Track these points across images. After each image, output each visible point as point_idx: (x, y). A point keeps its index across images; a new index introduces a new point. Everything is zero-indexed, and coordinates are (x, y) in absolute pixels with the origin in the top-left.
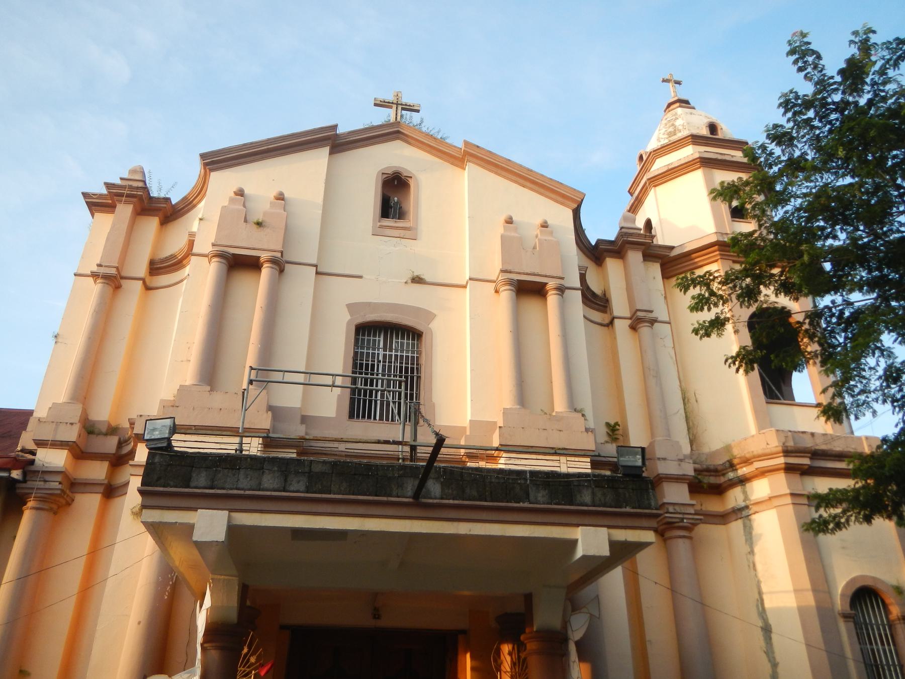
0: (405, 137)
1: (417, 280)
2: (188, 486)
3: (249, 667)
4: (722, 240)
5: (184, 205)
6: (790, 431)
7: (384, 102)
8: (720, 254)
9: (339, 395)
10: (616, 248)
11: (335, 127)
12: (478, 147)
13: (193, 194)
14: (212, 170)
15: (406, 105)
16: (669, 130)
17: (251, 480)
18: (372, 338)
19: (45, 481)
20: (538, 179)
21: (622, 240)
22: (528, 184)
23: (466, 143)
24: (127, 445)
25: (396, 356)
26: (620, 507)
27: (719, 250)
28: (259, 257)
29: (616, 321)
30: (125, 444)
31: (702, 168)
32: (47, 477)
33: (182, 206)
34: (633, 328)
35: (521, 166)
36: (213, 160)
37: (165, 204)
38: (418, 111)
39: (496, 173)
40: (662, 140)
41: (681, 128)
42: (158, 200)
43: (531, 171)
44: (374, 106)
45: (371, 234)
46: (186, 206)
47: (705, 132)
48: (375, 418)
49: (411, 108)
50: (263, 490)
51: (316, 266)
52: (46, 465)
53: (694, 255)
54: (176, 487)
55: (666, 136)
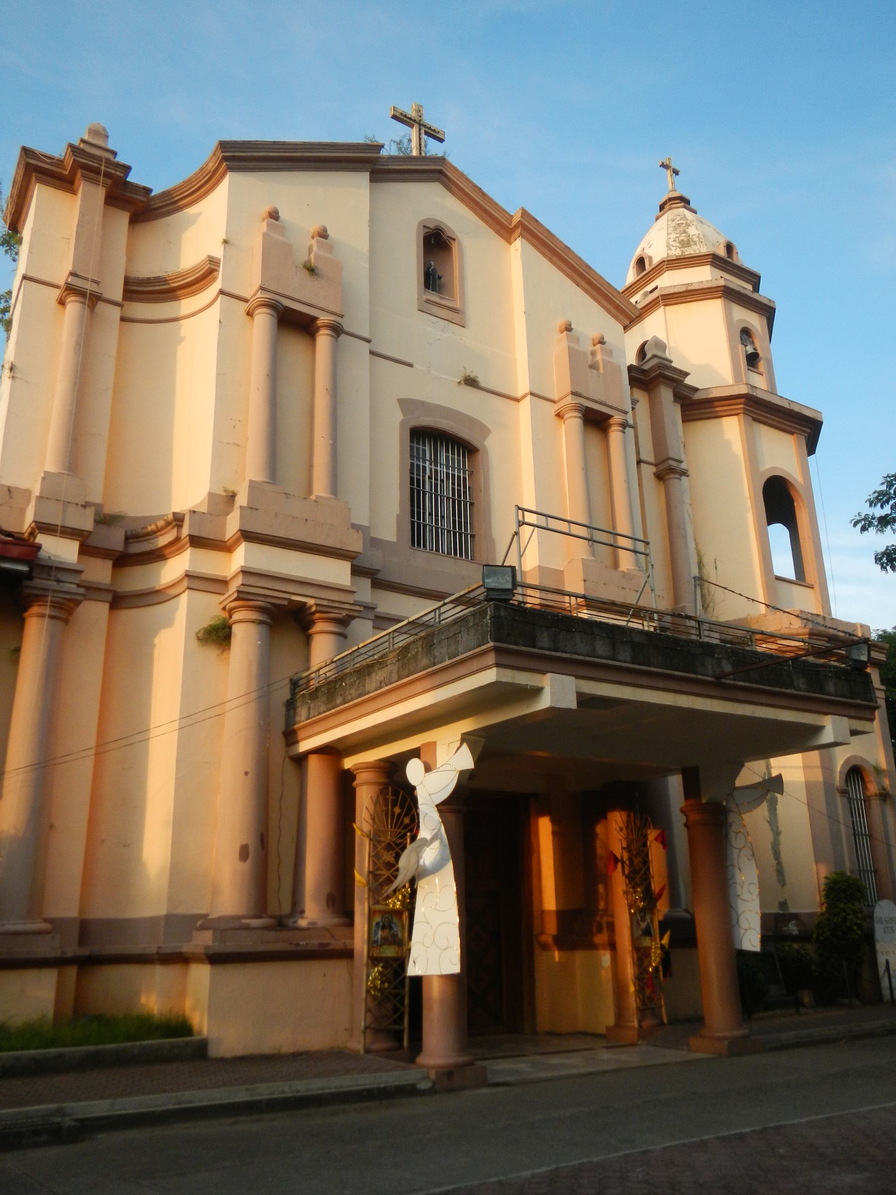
0: (447, 181)
1: (471, 382)
2: (534, 647)
3: (404, 829)
4: (751, 393)
5: (163, 204)
6: (809, 613)
7: (405, 116)
8: (744, 409)
9: (398, 515)
10: (647, 379)
12: (537, 221)
13: (181, 191)
14: (230, 169)
15: (430, 128)
16: (681, 238)
17: (586, 645)
18: (421, 447)
19: (58, 581)
20: (595, 280)
21: (657, 373)
22: (583, 284)
23: (524, 213)
24: (138, 542)
25: (448, 474)
26: (854, 699)
27: (744, 404)
28: (315, 319)
29: (643, 465)
30: (136, 540)
31: (723, 298)
32: (62, 576)
33: (160, 205)
34: (660, 477)
35: (580, 259)
36: (235, 154)
37: (145, 197)
38: (441, 140)
39: (550, 260)
40: (674, 248)
41: (696, 239)
42: (135, 188)
43: (590, 268)
44: (392, 118)
45: (416, 307)
46: (167, 205)
47: (722, 252)
48: (425, 546)
49: (434, 134)
50: (598, 657)
52: (52, 558)
53: (716, 403)
54: (525, 646)
55: (678, 245)
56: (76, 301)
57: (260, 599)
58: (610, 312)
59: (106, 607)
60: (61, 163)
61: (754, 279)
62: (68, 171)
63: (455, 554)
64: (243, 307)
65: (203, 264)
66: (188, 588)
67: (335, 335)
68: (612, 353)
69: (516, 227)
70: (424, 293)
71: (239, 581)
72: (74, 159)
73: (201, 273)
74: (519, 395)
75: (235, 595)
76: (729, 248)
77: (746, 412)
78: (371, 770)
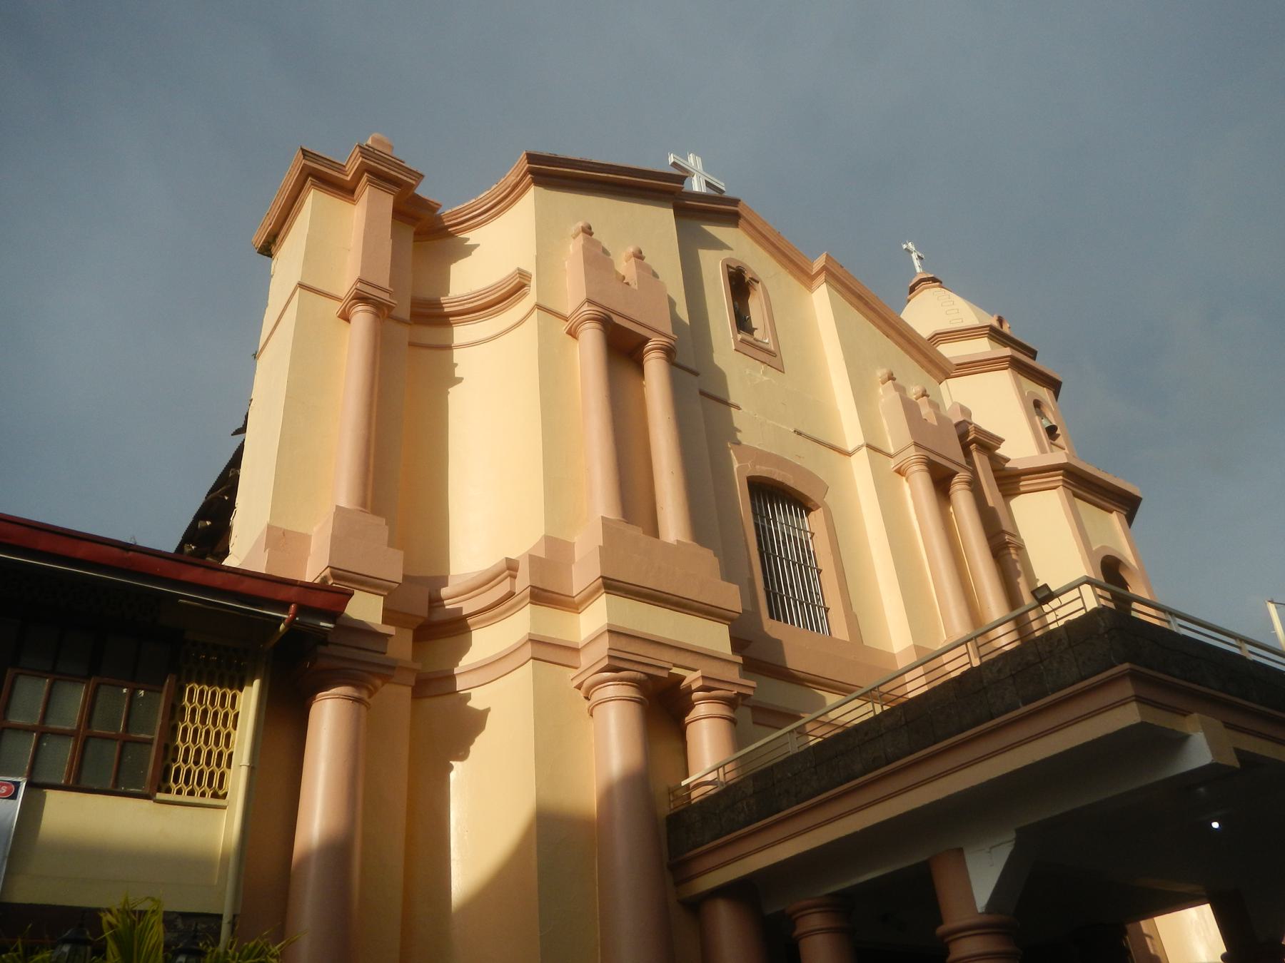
8: (1063, 481)
12: (842, 267)
27: (1063, 476)
51: (696, 374)
56: (366, 311)
57: (635, 667)
58: (922, 366)
59: (407, 691)
60: (341, 167)
61: (1032, 353)
62: (349, 178)
63: (812, 629)
64: (564, 327)
65: (511, 277)
68: (939, 407)
69: (818, 273)
70: (739, 333)
71: (604, 646)
72: (362, 161)
73: (505, 290)
74: (850, 448)
75: (606, 662)
76: (1000, 321)
77: (1066, 485)
78: (822, 909)
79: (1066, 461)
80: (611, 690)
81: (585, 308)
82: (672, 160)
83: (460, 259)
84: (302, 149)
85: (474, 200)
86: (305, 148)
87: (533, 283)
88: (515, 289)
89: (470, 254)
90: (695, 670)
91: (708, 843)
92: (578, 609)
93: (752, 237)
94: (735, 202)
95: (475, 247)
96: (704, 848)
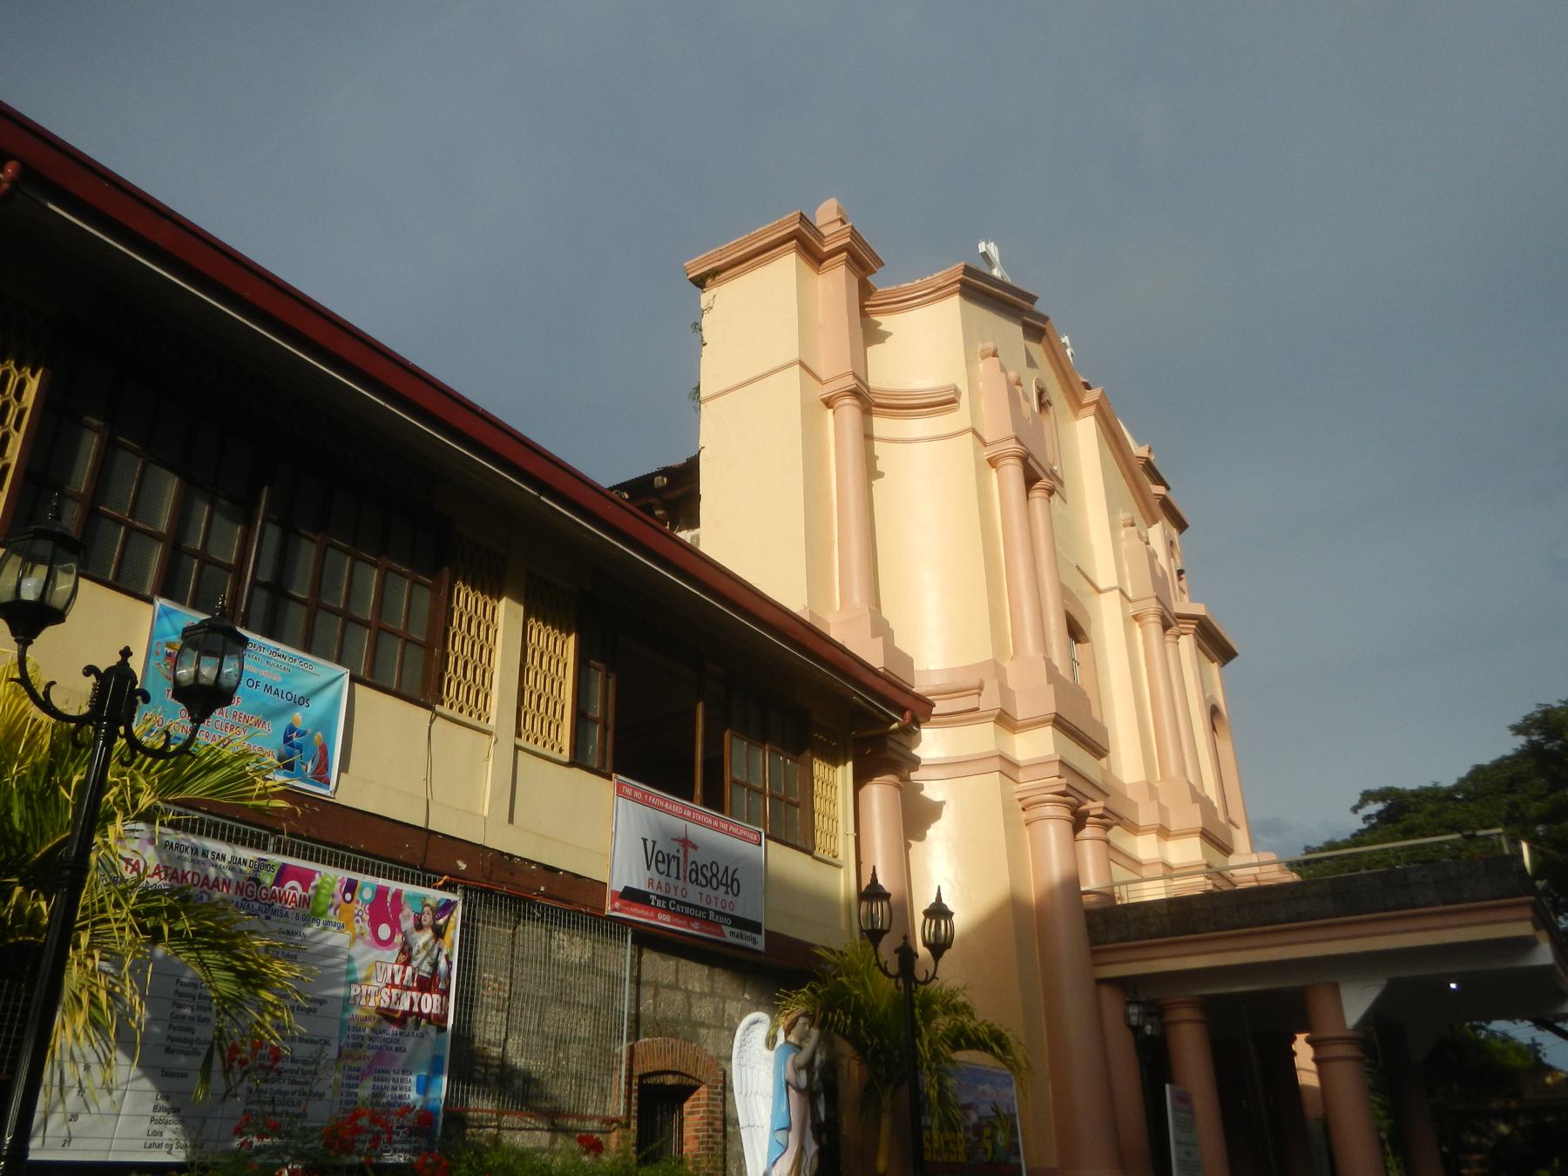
8: (1196, 630)
11: (1032, 299)
62: (825, 249)
66: (1000, 772)
67: (1046, 496)
69: (1089, 404)
74: (1101, 586)
75: (1063, 788)
79: (1203, 614)
80: (1049, 810)
81: (1012, 446)
82: (984, 250)
83: (876, 344)
84: (801, 214)
85: (895, 287)
86: (804, 213)
87: (964, 400)
88: (945, 402)
89: (884, 342)
90: (1094, 801)
91: (1112, 942)
92: (1015, 730)
93: (1048, 357)
94: (1045, 319)
95: (889, 334)
96: (1104, 946)
